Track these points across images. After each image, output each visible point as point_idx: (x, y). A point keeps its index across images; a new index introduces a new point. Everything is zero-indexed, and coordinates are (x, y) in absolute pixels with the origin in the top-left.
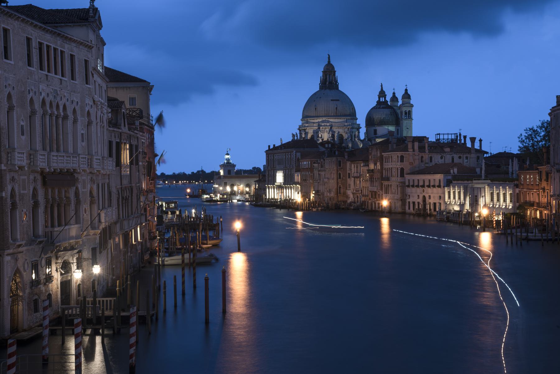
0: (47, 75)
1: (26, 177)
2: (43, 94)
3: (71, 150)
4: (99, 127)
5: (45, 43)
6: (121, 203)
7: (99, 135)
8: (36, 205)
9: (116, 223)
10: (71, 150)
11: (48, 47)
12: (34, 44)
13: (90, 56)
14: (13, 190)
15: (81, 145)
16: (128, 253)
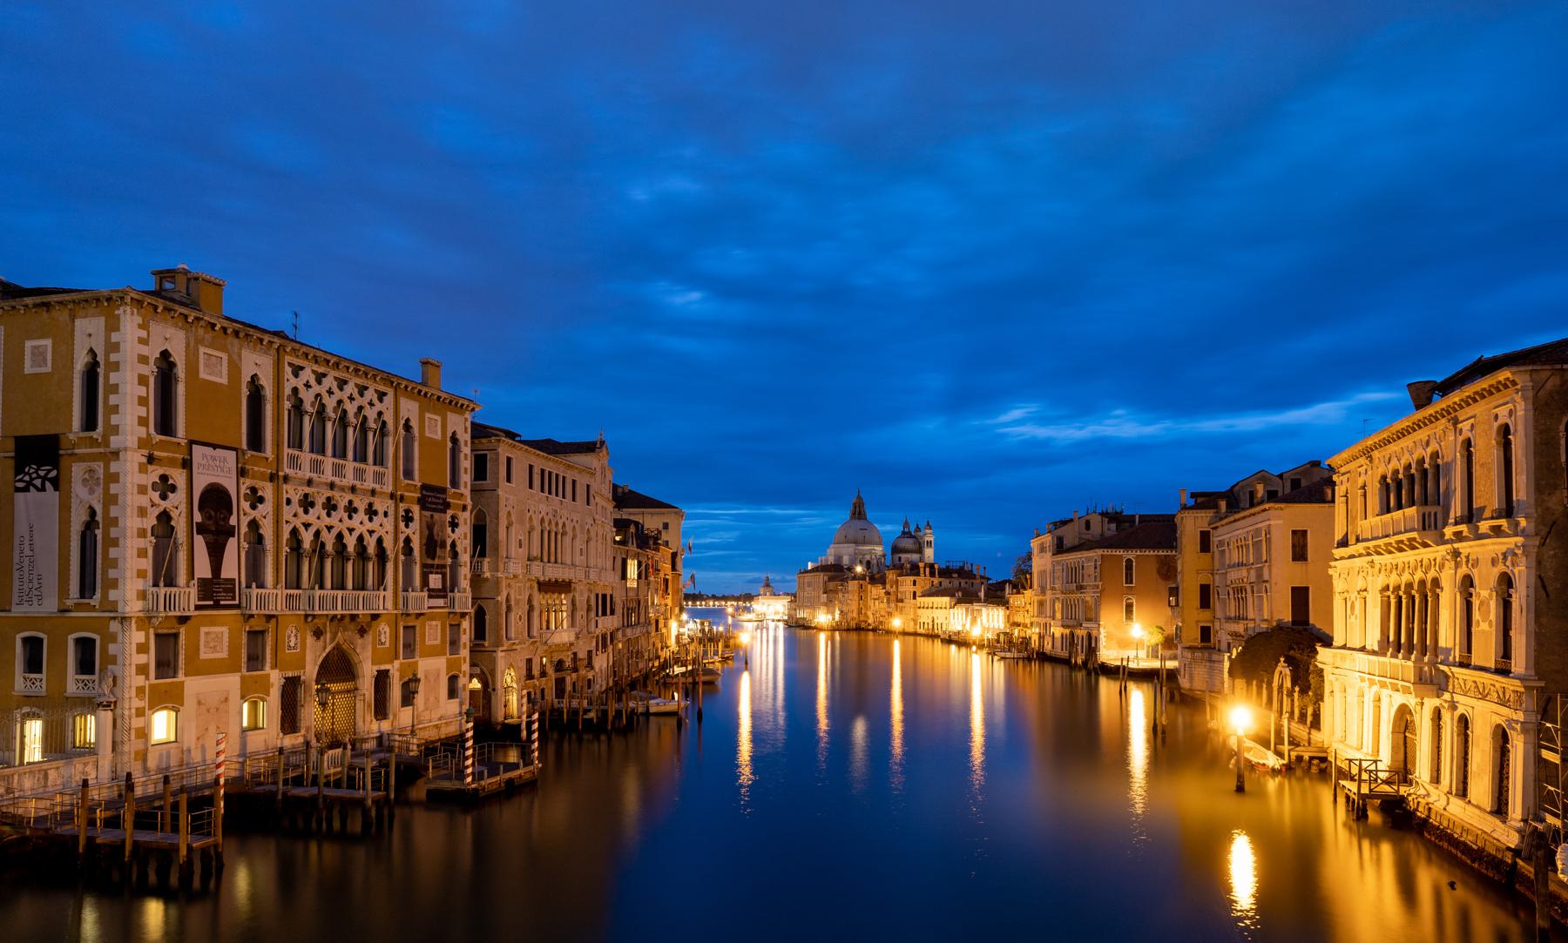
2: (542, 513)
3: (568, 561)
4: (600, 546)
5: (548, 469)
7: (599, 550)
8: (531, 609)
9: (618, 630)
10: (568, 561)
11: (550, 473)
12: (536, 471)
15: (579, 559)
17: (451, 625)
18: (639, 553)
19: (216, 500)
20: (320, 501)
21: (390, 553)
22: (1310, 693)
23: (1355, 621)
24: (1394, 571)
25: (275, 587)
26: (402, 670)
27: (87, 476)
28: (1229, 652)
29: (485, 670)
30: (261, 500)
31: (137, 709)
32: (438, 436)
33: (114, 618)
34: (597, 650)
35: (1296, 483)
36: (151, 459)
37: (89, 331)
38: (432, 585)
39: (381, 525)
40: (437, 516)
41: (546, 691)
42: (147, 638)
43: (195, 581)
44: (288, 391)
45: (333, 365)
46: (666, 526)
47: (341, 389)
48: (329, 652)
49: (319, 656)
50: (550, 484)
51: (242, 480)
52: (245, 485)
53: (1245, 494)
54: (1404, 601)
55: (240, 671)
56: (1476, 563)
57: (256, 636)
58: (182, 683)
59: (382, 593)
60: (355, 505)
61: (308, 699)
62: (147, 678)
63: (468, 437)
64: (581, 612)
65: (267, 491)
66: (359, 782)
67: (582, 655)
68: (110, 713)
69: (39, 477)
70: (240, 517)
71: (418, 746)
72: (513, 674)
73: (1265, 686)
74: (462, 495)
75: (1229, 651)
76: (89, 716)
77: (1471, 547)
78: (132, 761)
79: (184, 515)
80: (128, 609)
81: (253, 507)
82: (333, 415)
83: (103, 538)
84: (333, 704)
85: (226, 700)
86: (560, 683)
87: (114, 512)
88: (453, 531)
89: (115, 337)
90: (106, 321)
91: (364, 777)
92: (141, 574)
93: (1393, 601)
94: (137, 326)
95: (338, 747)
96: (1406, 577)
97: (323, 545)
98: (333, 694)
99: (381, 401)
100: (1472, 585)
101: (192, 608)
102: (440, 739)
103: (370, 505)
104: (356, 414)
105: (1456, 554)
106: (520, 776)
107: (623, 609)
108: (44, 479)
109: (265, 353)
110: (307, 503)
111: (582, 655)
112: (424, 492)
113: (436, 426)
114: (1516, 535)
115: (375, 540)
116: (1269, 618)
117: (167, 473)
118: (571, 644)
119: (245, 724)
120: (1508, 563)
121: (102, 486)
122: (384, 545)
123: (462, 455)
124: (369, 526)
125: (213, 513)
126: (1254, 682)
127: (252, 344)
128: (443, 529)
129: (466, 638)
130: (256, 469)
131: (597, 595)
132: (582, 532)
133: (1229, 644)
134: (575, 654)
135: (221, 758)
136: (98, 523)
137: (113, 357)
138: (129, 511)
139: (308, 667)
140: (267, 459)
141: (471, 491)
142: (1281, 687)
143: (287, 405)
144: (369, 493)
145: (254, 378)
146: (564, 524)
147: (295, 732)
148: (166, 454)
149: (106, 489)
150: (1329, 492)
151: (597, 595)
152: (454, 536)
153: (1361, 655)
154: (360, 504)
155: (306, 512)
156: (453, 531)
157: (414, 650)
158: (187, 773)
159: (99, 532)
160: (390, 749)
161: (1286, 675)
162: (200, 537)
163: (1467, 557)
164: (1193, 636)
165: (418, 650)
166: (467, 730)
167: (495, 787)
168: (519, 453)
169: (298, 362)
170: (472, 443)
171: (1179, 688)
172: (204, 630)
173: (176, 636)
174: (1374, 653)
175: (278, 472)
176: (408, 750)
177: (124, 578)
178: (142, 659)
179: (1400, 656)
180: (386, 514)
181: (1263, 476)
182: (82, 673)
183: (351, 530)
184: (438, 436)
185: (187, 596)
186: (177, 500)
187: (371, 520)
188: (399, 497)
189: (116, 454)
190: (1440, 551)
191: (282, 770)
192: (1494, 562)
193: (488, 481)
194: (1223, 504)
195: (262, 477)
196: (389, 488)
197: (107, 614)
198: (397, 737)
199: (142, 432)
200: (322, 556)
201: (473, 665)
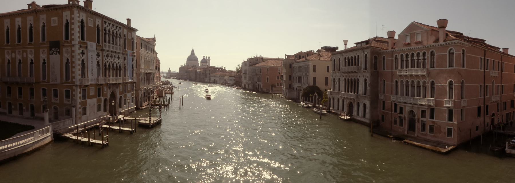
12: (146, 46)
69: (55, 51)
74: (134, 53)
80: (77, 84)
81: (98, 58)
89: (73, 16)
103: (118, 56)
108: (56, 52)
110: (107, 56)
124: (119, 61)
129: (135, 88)
137: (72, 21)
141: (136, 51)
149: (71, 54)
154: (117, 56)
159: (70, 65)
183: (115, 62)
189: (73, 46)
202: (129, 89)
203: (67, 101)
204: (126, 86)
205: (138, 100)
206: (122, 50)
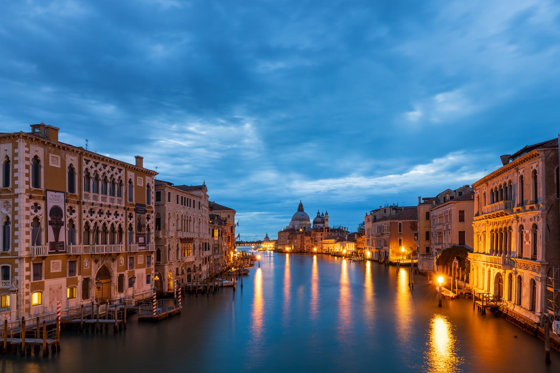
0: (184, 207)
1: (174, 240)
3: (192, 231)
4: (204, 224)
5: (184, 197)
6: (214, 249)
7: (204, 226)
8: (178, 249)
9: (211, 256)
10: (192, 231)
11: (185, 198)
12: (180, 197)
13: (201, 200)
14: (169, 244)
15: (196, 230)
16: (216, 266)
17: (147, 256)
18: (218, 227)
19: (56, 212)
20: (97, 210)
21: (124, 230)
22: (465, 270)
23: (481, 243)
24: (495, 224)
25: (79, 244)
26: (129, 274)
27: (5, 204)
28: (436, 256)
29: (160, 272)
30: (74, 211)
31: (26, 293)
32: (142, 185)
33: (17, 258)
34: (203, 264)
35: (460, 194)
36: (31, 197)
37: (6, 149)
38: (140, 242)
39: (120, 220)
40: (142, 215)
41: (184, 280)
42: (30, 265)
43: (49, 243)
44: (84, 170)
45: (101, 159)
46: (229, 216)
47: (105, 168)
48: (101, 268)
49: (97, 270)
50: (185, 202)
51: (66, 204)
52: (68, 206)
53: (442, 198)
54: (499, 235)
55: (66, 277)
56: (524, 221)
57: (72, 263)
58: (44, 282)
59: (121, 245)
60: (110, 212)
61: (93, 286)
62: (30, 280)
63: (153, 185)
64: (197, 250)
65: (76, 208)
66: (113, 316)
67: (197, 266)
68: (15, 294)
70: (65, 220)
71: (135, 302)
72: (171, 274)
73: (449, 268)
74: (151, 207)
75: (436, 255)
76: (7, 296)
77: (522, 215)
78: (24, 312)
79: (44, 218)
81: (71, 214)
82: (101, 178)
83: (12, 228)
84: (102, 288)
85: (61, 288)
86: (189, 276)
87: (16, 218)
88: (148, 221)
90: (12, 145)
91: (114, 315)
92: (27, 241)
93: (495, 235)
94: (25, 146)
95: (104, 304)
96: (500, 226)
97: (98, 227)
98: (102, 284)
99: (120, 172)
100: (523, 229)
101: (47, 253)
102: (143, 299)
103: (116, 212)
104: (110, 177)
105: (517, 217)
106: (174, 312)
107: (213, 248)
109: (75, 155)
110: (92, 212)
111: (197, 266)
112: (137, 207)
113: (141, 181)
114: (539, 210)
115: (118, 225)
116: (451, 243)
117: (37, 202)
118: (193, 262)
119: (68, 296)
120: (536, 220)
121: (11, 208)
122: (122, 227)
123: (151, 192)
124: (116, 220)
125: (55, 217)
126: (445, 267)
127: (70, 152)
128: (144, 220)
129: (153, 261)
130: (72, 199)
131: (203, 243)
132: (197, 220)
133: (436, 253)
134: (195, 265)
135: (59, 310)
136: (10, 222)
137: (16, 159)
138: (22, 217)
139: (93, 274)
140: (76, 196)
141: (155, 205)
142: (455, 268)
143: (84, 175)
144: (116, 207)
145: (71, 165)
146: (190, 217)
147: (88, 299)
148: (37, 195)
150: (472, 196)
151: (203, 243)
152: (148, 223)
153: (483, 255)
154: (113, 212)
155: (91, 215)
156: (148, 221)
157: (133, 266)
158: (46, 316)
159: (10, 226)
160: (125, 304)
161: (457, 264)
162: (50, 226)
163: (521, 218)
164: (423, 250)
165: (135, 266)
166: (154, 296)
167: (164, 316)
168: (173, 190)
169: (88, 158)
170: (155, 187)
171: (418, 270)
172: (52, 261)
173: (41, 264)
174: (488, 254)
175: (80, 200)
176: (131, 304)
177: (21, 243)
178: (28, 273)
179: (497, 255)
180: (122, 215)
181: (449, 191)
182: (4, 280)
183: (109, 222)
184: (142, 185)
185: (45, 249)
186: (41, 212)
187: (116, 217)
188: (127, 209)
189: (17, 196)
190: (512, 217)
191: (83, 314)
192: (531, 220)
193: (161, 202)
194: (434, 202)
195: (74, 202)
196: (123, 205)
197: (14, 257)
198: (127, 299)
199: (27, 187)
200: (98, 232)
201: (156, 271)
202: (139, 263)
203: (4, 284)
204: (133, 257)
205: (164, 280)
206: (124, 203)
